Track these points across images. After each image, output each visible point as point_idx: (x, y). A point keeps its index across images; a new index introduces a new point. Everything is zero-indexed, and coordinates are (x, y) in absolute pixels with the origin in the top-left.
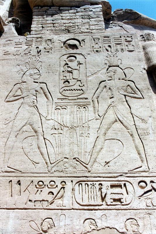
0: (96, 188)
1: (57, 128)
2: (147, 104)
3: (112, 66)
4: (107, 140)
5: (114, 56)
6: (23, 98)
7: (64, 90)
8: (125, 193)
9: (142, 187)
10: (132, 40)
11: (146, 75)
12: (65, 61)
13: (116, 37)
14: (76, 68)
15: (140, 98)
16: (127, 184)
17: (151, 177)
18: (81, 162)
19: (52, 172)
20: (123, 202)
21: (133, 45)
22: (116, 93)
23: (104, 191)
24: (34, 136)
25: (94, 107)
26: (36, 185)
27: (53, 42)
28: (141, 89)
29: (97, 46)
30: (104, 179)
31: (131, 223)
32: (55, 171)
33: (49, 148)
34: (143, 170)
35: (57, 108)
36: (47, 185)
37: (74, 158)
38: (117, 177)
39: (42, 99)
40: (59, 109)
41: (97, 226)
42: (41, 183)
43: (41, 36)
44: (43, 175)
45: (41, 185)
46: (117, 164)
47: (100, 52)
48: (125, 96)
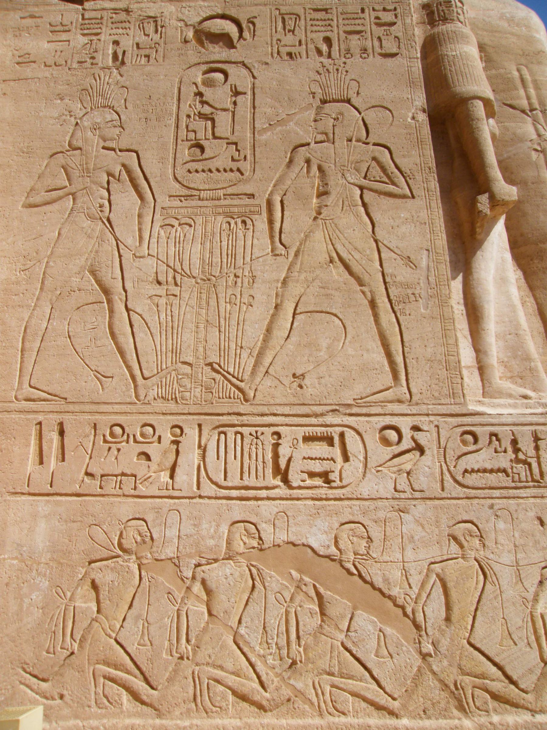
0: (262, 444)
2: (421, 214)
3: (330, 102)
4: (301, 313)
6: (73, 194)
7: (189, 171)
8: (339, 459)
10: (395, 20)
11: (426, 131)
13: (350, 9)
14: (225, 106)
15: (404, 197)
17: (414, 415)
19: (146, 401)
20: (334, 481)
21: (396, 37)
22: (336, 182)
23: (284, 451)
24: (100, 302)
25: (271, 222)
26: (104, 436)
27: (162, 27)
28: (408, 172)
29: (289, 39)
31: (351, 533)
32: (155, 399)
34: (395, 398)
35: (167, 222)
36: (134, 436)
37: (210, 364)
38: (322, 415)
39: (126, 199)
40: (173, 226)
41: (260, 538)
42: (118, 430)
43: (125, 6)
44: (124, 408)
45: (118, 433)
46: (323, 381)
47: (298, 56)
48: (361, 188)
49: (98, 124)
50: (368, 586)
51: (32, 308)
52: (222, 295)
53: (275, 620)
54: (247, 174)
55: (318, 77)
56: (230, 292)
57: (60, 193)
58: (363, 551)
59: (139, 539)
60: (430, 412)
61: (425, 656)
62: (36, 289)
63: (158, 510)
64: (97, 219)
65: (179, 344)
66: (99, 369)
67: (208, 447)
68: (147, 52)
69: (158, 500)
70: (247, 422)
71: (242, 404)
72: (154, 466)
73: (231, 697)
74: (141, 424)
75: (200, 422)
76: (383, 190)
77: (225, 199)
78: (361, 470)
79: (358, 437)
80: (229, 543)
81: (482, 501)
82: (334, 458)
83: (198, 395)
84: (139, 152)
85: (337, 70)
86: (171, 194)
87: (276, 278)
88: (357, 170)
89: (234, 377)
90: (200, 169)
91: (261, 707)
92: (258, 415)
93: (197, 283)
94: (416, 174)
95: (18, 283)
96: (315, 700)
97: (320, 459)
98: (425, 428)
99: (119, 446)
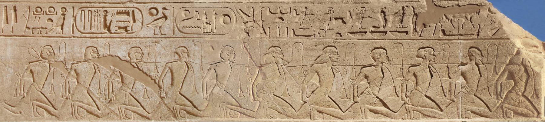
8: (132, 21)
9: (151, 14)
23: (109, 18)
30: (110, 5)
42: (39, 9)
45: (39, 11)
50: (141, 72)
53: (104, 85)
58: (140, 58)
59: (49, 53)
61: (162, 98)
63: (56, 42)
69: (56, 38)
72: (54, 24)
73: (86, 113)
78: (140, 26)
79: (140, 12)
80: (85, 55)
81: (190, 39)
91: (98, 116)
96: (118, 114)
99: (40, 16)
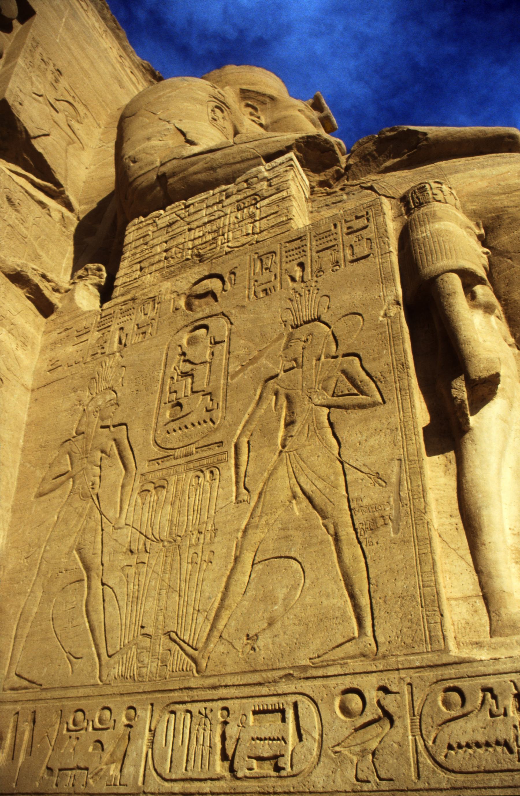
0: (211, 724)
1: (134, 548)
3: (301, 325)
4: (259, 562)
5: (309, 291)
12: (180, 346)
16: (305, 704)
17: (381, 671)
18: (182, 643)
20: (284, 769)
21: (367, 239)
23: (232, 731)
25: (237, 466)
26: (67, 723)
33: (109, 609)
36: (93, 721)
37: (168, 634)
39: (115, 472)
46: (277, 640)
49: (99, 406)
51: (27, 595)
52: (185, 556)
54: (218, 422)
55: (289, 305)
56: (192, 551)
57: (63, 478)
60: (400, 666)
62: (33, 575)
64: (88, 497)
65: (141, 615)
66: (73, 651)
67: (157, 730)
68: (143, 330)
70: (196, 698)
71: (194, 676)
72: (106, 757)
74: (100, 708)
75: (152, 702)
76: (352, 403)
77: (197, 452)
78: (315, 752)
82: (285, 737)
83: (154, 670)
84: (128, 425)
85: (309, 291)
86: (150, 459)
87: (236, 528)
88: (325, 389)
89: (189, 645)
90: (177, 429)
92: (209, 688)
93: (164, 546)
94: (387, 375)
95: (20, 571)
97: (270, 739)
98: (394, 688)
